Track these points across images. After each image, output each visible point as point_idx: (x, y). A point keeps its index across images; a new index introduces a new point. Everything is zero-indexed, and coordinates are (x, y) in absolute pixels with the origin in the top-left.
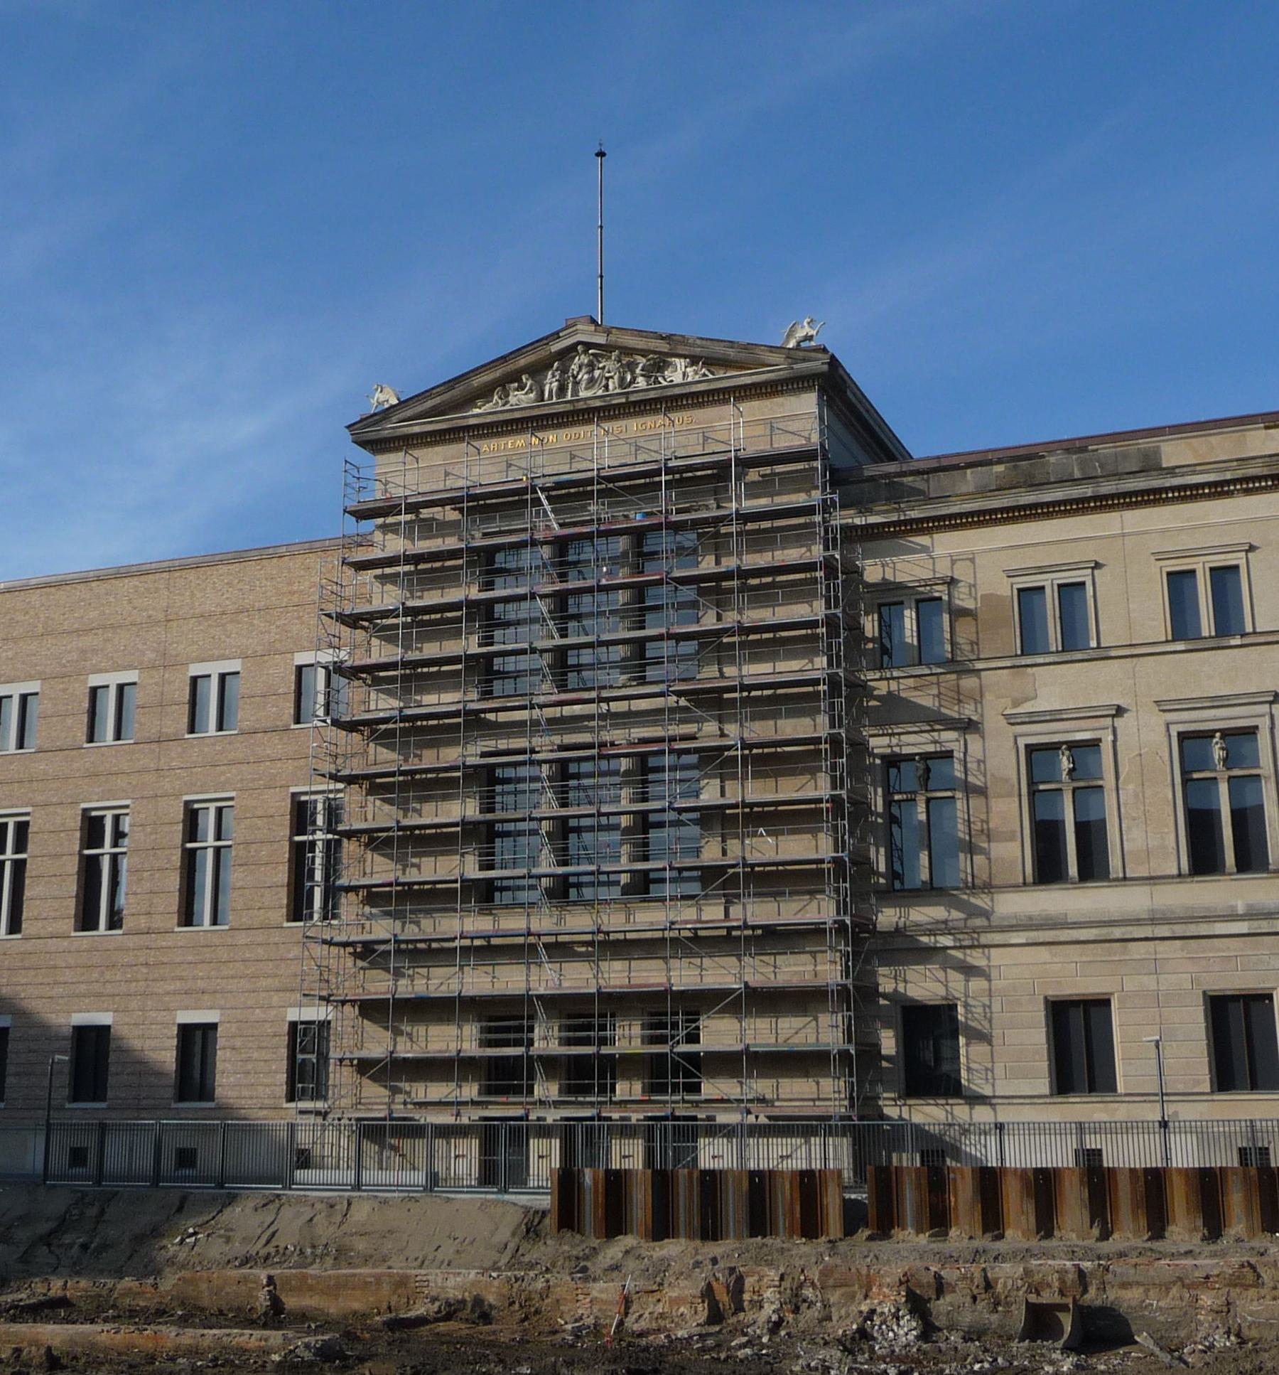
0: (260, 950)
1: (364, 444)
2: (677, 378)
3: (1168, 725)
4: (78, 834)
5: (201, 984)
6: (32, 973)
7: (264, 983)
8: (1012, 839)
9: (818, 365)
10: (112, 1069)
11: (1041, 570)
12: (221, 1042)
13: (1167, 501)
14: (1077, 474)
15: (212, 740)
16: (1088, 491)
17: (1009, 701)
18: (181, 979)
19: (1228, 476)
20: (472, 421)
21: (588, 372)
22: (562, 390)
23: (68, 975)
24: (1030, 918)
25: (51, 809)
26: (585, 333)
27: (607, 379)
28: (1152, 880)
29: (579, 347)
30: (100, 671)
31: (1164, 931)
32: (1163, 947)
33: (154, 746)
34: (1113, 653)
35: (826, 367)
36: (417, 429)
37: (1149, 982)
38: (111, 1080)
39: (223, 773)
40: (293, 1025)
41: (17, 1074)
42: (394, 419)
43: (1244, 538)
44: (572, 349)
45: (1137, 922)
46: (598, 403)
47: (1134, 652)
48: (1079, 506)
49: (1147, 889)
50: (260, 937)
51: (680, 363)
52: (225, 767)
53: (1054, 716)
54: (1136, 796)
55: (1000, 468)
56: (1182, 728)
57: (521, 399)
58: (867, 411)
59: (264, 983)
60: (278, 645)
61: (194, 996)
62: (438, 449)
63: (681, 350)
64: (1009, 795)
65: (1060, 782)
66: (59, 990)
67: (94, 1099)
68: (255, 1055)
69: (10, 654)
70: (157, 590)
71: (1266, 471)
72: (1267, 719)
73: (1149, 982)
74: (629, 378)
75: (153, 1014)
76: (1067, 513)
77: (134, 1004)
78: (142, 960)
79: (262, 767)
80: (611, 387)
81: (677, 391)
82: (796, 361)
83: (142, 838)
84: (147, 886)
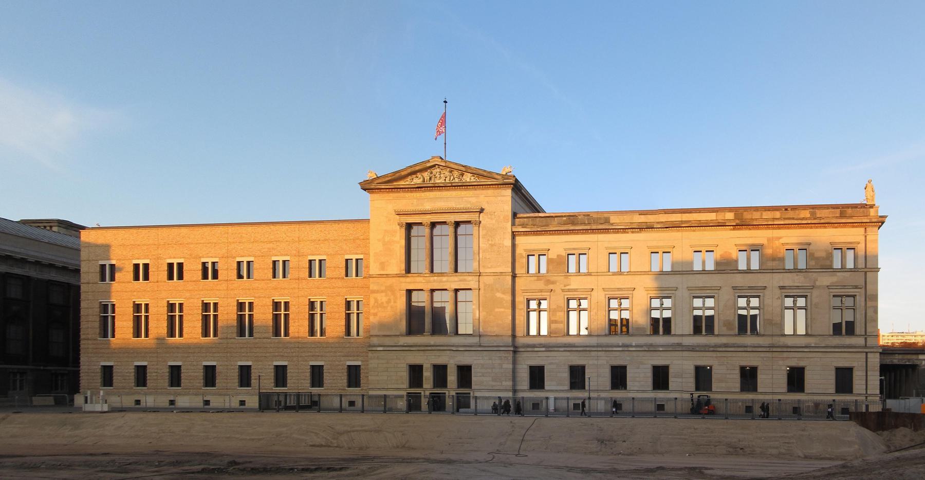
0: (337, 345)
1: (365, 190)
2: (468, 180)
3: (605, 295)
4: (272, 307)
5: (317, 354)
6: (258, 349)
8: (562, 323)
9: (512, 181)
10: (288, 378)
11: (574, 249)
12: (325, 371)
15: (316, 281)
16: (588, 227)
17: (563, 285)
21: (439, 175)
22: (430, 179)
24: (565, 344)
25: (261, 299)
26: (438, 162)
27: (446, 177)
29: (437, 166)
31: (600, 349)
32: (600, 353)
35: (514, 182)
36: (383, 187)
37: (595, 362)
38: (288, 381)
40: (349, 366)
43: (629, 245)
44: (434, 166)
45: (594, 347)
48: (586, 231)
51: (470, 175)
52: (323, 289)
53: (575, 290)
57: (417, 180)
61: (316, 357)
62: (391, 194)
63: (469, 171)
64: (561, 311)
66: (268, 354)
68: (336, 374)
72: (631, 295)
73: (595, 362)
74: (452, 177)
75: (302, 362)
76: (583, 233)
77: (295, 359)
80: (447, 180)
83: (295, 309)
84: (297, 324)
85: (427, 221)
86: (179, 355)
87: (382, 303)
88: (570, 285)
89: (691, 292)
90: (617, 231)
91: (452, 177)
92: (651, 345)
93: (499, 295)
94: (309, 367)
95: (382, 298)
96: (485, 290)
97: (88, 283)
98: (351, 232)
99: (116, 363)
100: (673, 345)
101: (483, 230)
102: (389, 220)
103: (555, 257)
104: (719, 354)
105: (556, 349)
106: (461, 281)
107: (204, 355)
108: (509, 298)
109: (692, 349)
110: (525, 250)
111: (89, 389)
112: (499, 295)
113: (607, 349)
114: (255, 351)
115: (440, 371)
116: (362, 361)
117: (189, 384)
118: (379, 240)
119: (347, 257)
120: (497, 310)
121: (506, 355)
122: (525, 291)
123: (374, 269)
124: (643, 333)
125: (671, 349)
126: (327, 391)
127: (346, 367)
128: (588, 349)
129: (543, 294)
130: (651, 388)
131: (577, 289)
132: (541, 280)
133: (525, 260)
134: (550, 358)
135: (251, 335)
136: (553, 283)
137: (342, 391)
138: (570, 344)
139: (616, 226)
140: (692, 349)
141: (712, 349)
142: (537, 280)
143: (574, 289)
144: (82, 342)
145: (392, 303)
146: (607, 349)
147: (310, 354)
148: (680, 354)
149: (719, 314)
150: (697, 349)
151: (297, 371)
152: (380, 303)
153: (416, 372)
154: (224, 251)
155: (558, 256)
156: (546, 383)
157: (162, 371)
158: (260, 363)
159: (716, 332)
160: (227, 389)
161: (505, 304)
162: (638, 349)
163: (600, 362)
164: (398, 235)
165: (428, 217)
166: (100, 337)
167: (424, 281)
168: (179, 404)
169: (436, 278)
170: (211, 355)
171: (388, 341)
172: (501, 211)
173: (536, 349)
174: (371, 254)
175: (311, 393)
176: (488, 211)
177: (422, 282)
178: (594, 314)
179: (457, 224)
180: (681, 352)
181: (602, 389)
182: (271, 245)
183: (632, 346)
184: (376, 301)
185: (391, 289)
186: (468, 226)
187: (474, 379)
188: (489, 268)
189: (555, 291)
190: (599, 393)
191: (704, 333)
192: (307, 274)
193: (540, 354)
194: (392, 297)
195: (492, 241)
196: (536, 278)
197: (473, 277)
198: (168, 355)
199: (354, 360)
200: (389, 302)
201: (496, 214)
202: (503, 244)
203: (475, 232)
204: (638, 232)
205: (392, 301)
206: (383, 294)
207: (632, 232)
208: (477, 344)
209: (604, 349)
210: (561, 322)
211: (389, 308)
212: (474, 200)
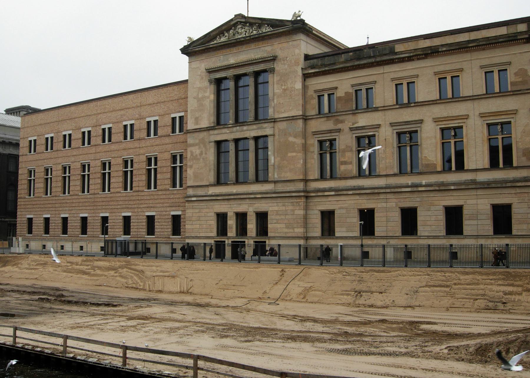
0: (164, 196)
2: (264, 31)
5: (151, 205)
7: (165, 205)
10: (132, 227)
13: (395, 63)
14: (372, 55)
16: (373, 60)
17: (351, 124)
18: (147, 204)
19: (412, 54)
20: (211, 46)
22: (234, 35)
23: (121, 203)
24: (354, 186)
25: (116, 158)
28: (387, 176)
30: (126, 121)
31: (388, 190)
33: (139, 141)
34: (379, 109)
37: (384, 205)
38: (131, 230)
39: (155, 148)
40: (174, 216)
41: (111, 228)
42: (192, 46)
44: (237, 23)
45: (382, 188)
46: (243, 39)
47: (385, 109)
49: (385, 178)
50: (164, 192)
53: (363, 128)
54: (384, 151)
55: (351, 54)
56: (397, 131)
58: (324, 36)
59: (165, 205)
60: (167, 112)
65: (365, 147)
66: (119, 207)
67: (152, 235)
68: (164, 224)
69: (105, 117)
70: (138, 97)
71: (422, 53)
73: (384, 205)
77: (136, 210)
78: (137, 199)
79: (164, 146)
81: (263, 35)
82: (295, 24)
85: (230, 75)
86: (67, 209)
87: (196, 155)
88: (358, 123)
89: (484, 119)
90: (402, 60)
91: (251, 30)
92: (443, 184)
93: (291, 139)
94: (145, 217)
95: (196, 151)
96: (279, 135)
97: (23, 155)
98: (176, 93)
99: (34, 216)
100: (466, 183)
101: (277, 76)
102: (202, 78)
103: (344, 95)
104: (518, 190)
105: (345, 192)
106: (258, 129)
107: (81, 208)
108: (299, 141)
109: (487, 186)
110: (315, 91)
111: (20, 236)
112: (291, 139)
113: (396, 190)
114: (111, 204)
115: (242, 217)
116: (182, 211)
117: (72, 233)
118: (194, 98)
119: (173, 116)
120: (290, 154)
121: (298, 201)
122: (315, 133)
123: (190, 125)
124: (433, 170)
125: (463, 187)
126: (156, 239)
127: (171, 216)
128: (376, 191)
129: (333, 134)
130: (443, 233)
131: (364, 126)
132: (330, 120)
133: (315, 101)
134: (340, 202)
135: (109, 191)
136: (342, 122)
137: (168, 239)
138: (359, 186)
139: (400, 54)
140: (487, 186)
141: (509, 185)
142: (327, 121)
143: (362, 127)
144: (19, 200)
145: (204, 155)
146: (396, 190)
147: (145, 205)
148: (474, 192)
149: (516, 141)
150: (493, 185)
151: (137, 221)
152: (194, 155)
153: (222, 218)
154: (95, 121)
155: (346, 93)
156: (337, 229)
157: (58, 222)
158: (114, 214)
159: (515, 164)
160: (93, 237)
161: (297, 148)
162: (429, 189)
163: (389, 205)
164: (209, 89)
165: (231, 70)
166: (27, 196)
167: (227, 132)
168: (66, 249)
169: (238, 128)
170: (85, 208)
171: (200, 192)
172: (293, 56)
173: (326, 194)
174: (188, 111)
175: (146, 240)
176: (281, 57)
177: (226, 133)
178: (383, 152)
179: (257, 74)
180: (475, 190)
181: (391, 235)
182: (122, 112)
183: (421, 186)
184: (192, 153)
185: (202, 141)
186: (266, 74)
187: (269, 226)
188: (283, 113)
189: (343, 130)
190: (388, 240)
191: (501, 165)
192: (146, 134)
193: (330, 199)
194: (204, 150)
195: (285, 86)
196: (325, 119)
197: (269, 123)
198: (61, 209)
199: (176, 211)
200: (201, 154)
201: (288, 59)
202: (294, 88)
203: (270, 80)
204: (423, 58)
205: (204, 152)
206: (197, 147)
207: (418, 59)
208: (272, 190)
209: (393, 190)
210: (351, 163)
211: (201, 160)
212: (269, 48)
